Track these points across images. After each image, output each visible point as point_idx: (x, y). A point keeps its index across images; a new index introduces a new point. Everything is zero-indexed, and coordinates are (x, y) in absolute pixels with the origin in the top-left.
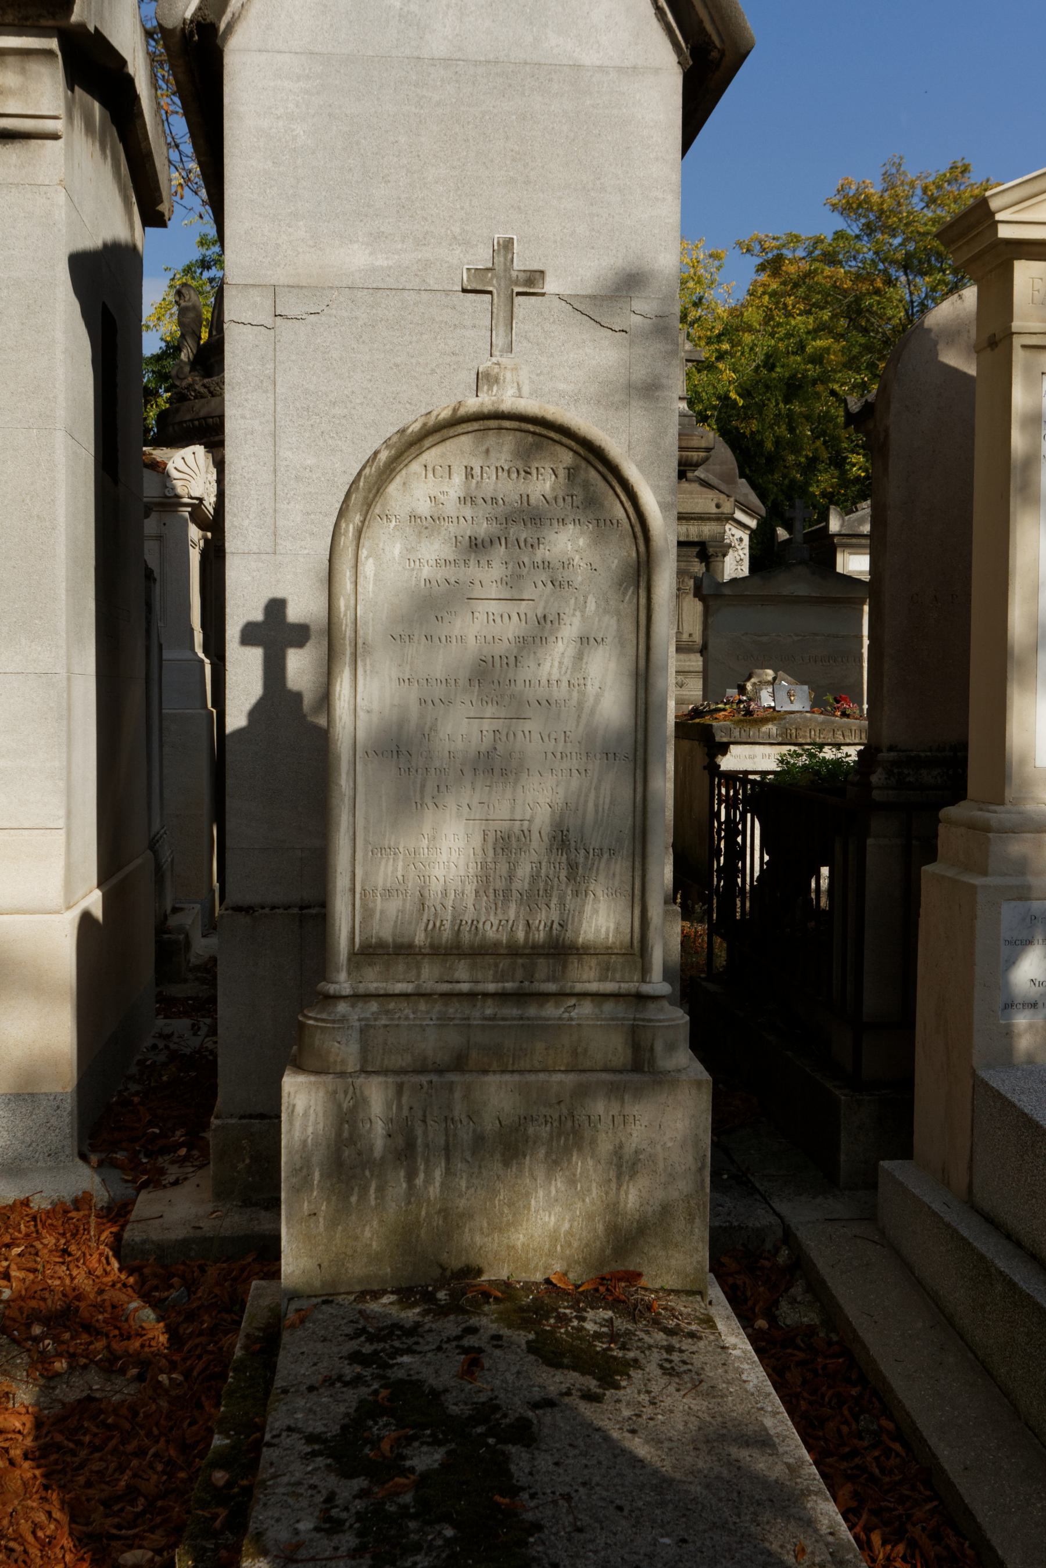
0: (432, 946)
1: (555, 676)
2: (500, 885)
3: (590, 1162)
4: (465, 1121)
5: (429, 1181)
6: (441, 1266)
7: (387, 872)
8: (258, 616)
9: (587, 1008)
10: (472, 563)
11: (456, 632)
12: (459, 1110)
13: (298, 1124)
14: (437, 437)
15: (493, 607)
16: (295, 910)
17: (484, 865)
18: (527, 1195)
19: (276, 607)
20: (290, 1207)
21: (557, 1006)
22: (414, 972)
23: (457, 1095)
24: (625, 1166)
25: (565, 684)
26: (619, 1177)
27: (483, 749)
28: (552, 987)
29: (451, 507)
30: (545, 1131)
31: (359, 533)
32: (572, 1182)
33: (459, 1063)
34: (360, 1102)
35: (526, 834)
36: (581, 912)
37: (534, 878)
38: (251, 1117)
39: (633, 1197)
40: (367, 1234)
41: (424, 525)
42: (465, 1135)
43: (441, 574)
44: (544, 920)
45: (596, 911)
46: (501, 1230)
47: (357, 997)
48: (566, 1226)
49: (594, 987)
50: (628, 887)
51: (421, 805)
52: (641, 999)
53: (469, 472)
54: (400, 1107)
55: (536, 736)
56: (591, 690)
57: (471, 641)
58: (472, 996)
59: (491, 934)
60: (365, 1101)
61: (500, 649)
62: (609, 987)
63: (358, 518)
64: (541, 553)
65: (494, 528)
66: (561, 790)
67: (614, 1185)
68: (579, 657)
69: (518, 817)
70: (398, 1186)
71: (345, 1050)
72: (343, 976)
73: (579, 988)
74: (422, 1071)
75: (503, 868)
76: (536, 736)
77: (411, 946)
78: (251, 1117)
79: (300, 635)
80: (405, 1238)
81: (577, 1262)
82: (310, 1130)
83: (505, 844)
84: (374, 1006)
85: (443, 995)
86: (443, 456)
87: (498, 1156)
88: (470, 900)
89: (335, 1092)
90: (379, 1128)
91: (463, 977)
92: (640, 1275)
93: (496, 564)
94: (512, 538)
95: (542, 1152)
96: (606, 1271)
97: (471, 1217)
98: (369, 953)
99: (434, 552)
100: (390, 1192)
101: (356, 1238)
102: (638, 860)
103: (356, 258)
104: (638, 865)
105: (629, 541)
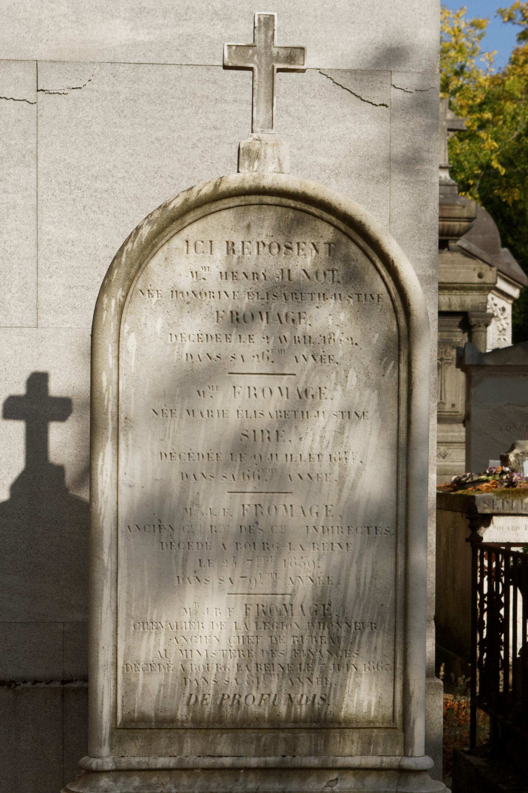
1: (316, 452)
2: (263, 659)
8: (21, 390)
10: (234, 337)
14: (199, 212)
15: (255, 381)
16: (58, 685)
17: (246, 639)
19: (38, 381)
21: (319, 780)
22: (175, 748)
25: (326, 458)
27: (245, 524)
28: (314, 761)
29: (213, 282)
35: (288, 608)
36: (343, 686)
37: (296, 652)
41: (187, 299)
43: (202, 348)
44: (305, 695)
45: (358, 685)
47: (121, 772)
49: (356, 761)
50: (390, 661)
51: (183, 579)
52: (403, 773)
53: (230, 248)
56: (353, 464)
57: (233, 416)
58: (234, 770)
59: (253, 708)
61: (261, 423)
62: (372, 761)
63: (120, 293)
64: (302, 328)
65: (256, 303)
66: (323, 564)
68: (341, 431)
69: (280, 590)
72: (105, 750)
73: (341, 761)
75: (265, 643)
76: (297, 510)
77: (173, 720)
79: (62, 408)
83: (267, 618)
85: (204, 769)
88: (232, 674)
91: (225, 751)
93: (257, 338)
94: (273, 313)
98: (133, 727)
99: (196, 325)
102: (400, 633)
103: (117, 34)
104: (399, 639)
105: (389, 316)
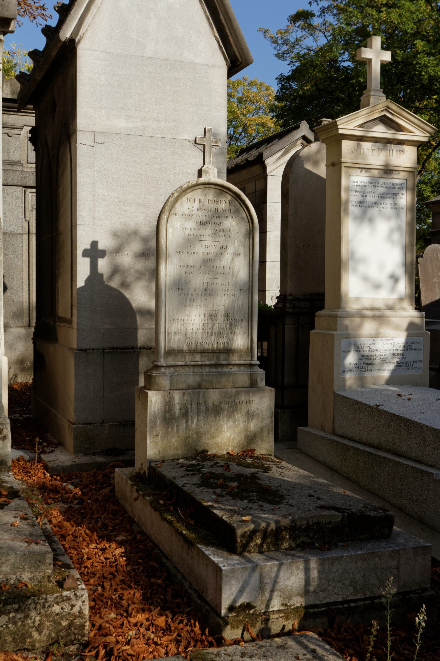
0: (189, 350)
1: (225, 266)
2: (209, 331)
3: (240, 415)
4: (203, 404)
5: (192, 423)
6: (196, 450)
7: (174, 327)
8: (88, 247)
9: (235, 369)
10: (201, 229)
11: (196, 251)
12: (201, 401)
13: (153, 406)
14: (191, 189)
15: (208, 243)
16: (101, 351)
17: (204, 325)
18: (221, 427)
19: (94, 244)
20: (150, 433)
21: (227, 368)
22: (183, 359)
23: (201, 396)
24: (250, 415)
25: (228, 268)
26: (248, 420)
27: (204, 288)
28: (225, 362)
29: (195, 212)
30: (226, 406)
31: (168, 219)
32: (234, 422)
33: (199, 386)
34: (172, 398)
35: (217, 315)
36: (233, 339)
37: (219, 328)
38: (86, 424)
39: (253, 426)
40: (174, 441)
41: (188, 216)
42: (203, 408)
43: (192, 232)
44: (223, 341)
45: (237, 339)
46: (214, 438)
47: (167, 367)
48: (233, 436)
49: (238, 362)
50: (247, 331)
51: (185, 306)
52: (251, 365)
53: (200, 201)
54: (184, 400)
55: (220, 284)
56: (236, 270)
57: (201, 254)
58: (201, 365)
59: (206, 346)
60: (173, 398)
61: (210, 256)
62: (242, 362)
63: (167, 214)
64: (221, 227)
65: (208, 218)
66: (227, 301)
67: (247, 422)
68: (233, 259)
69: (214, 309)
70: (183, 425)
71: (165, 382)
72: (162, 360)
73: (233, 362)
74: (189, 389)
75: (210, 326)
76: (220, 284)
77: (182, 350)
78: (86, 424)
79: (103, 254)
80: (186, 442)
81: (236, 447)
82: (156, 408)
83: (212, 317)
84: (172, 369)
85: (192, 365)
86: (192, 195)
87: (213, 415)
88: (200, 335)
89: (164, 396)
90: (177, 407)
91: (198, 359)
92: (255, 450)
93: (208, 230)
94: (213, 222)
95: (226, 413)
96: (244, 449)
97: (205, 434)
98: (170, 353)
99: (190, 225)
100: (181, 427)
101: (170, 442)
102: (250, 322)
103: (121, 124)
104: (250, 324)
105: (247, 224)
